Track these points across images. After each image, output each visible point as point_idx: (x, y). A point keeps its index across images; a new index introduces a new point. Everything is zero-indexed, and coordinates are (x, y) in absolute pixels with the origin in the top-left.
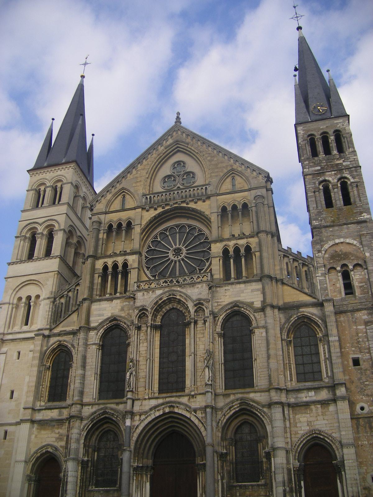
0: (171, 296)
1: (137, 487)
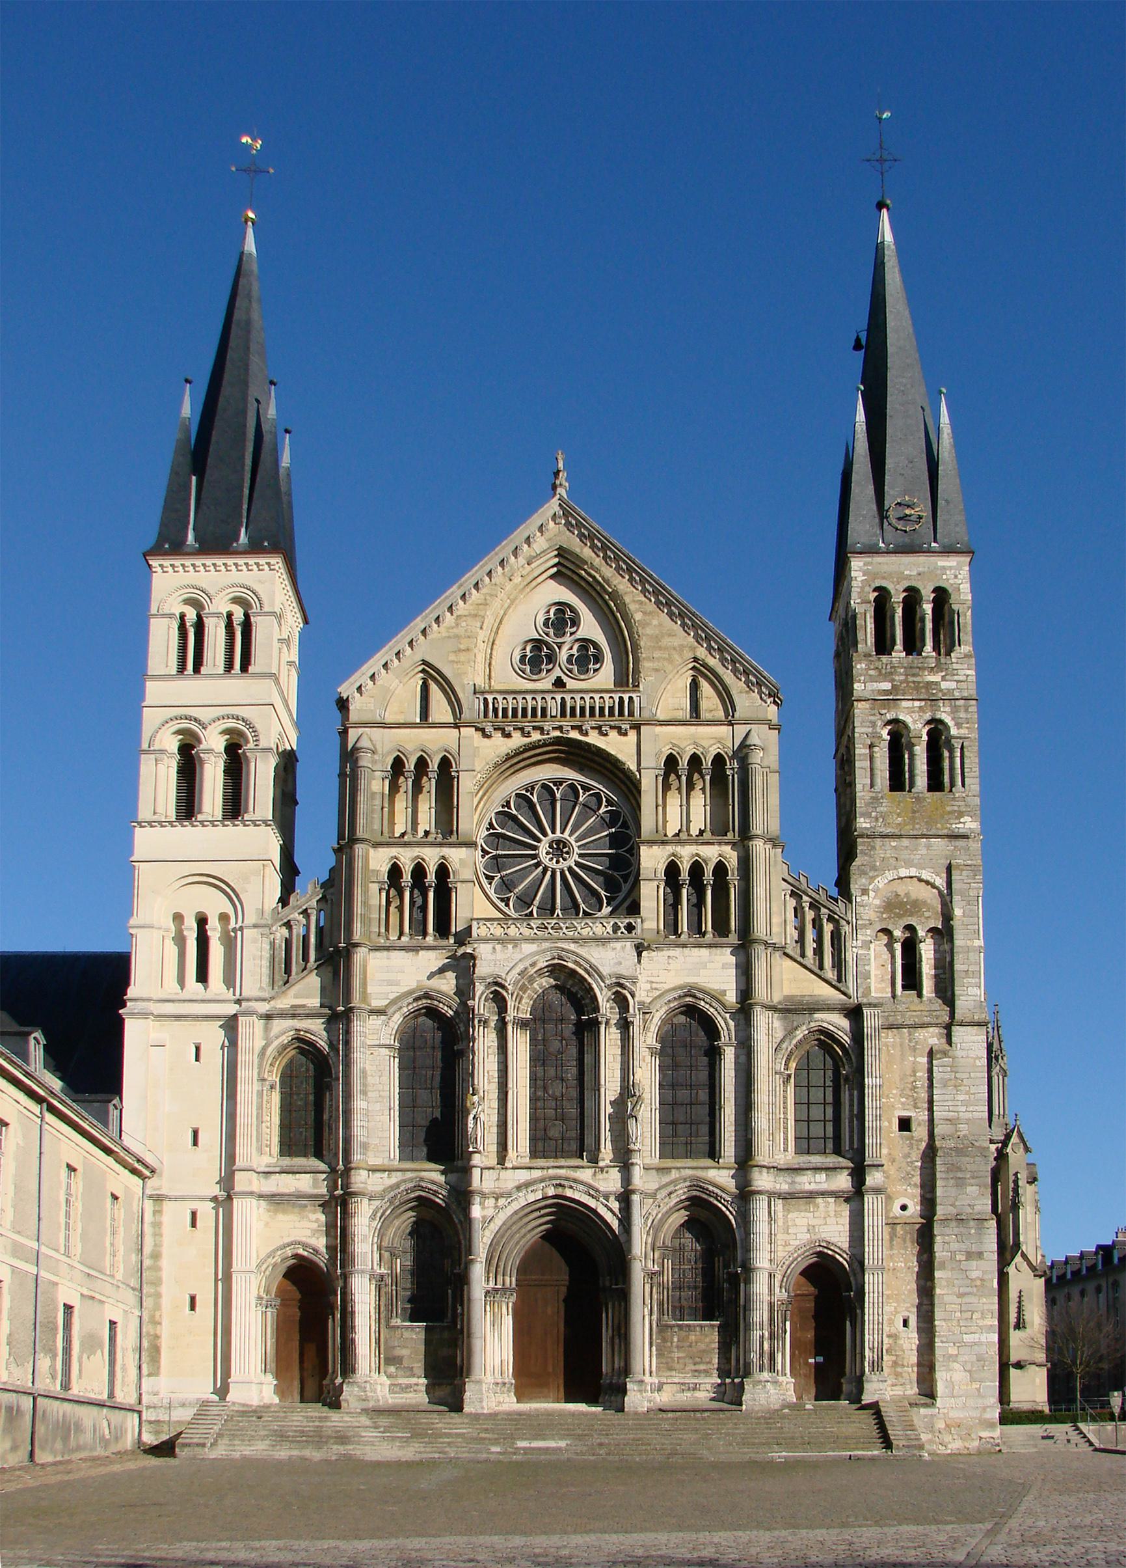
0: (556, 961)
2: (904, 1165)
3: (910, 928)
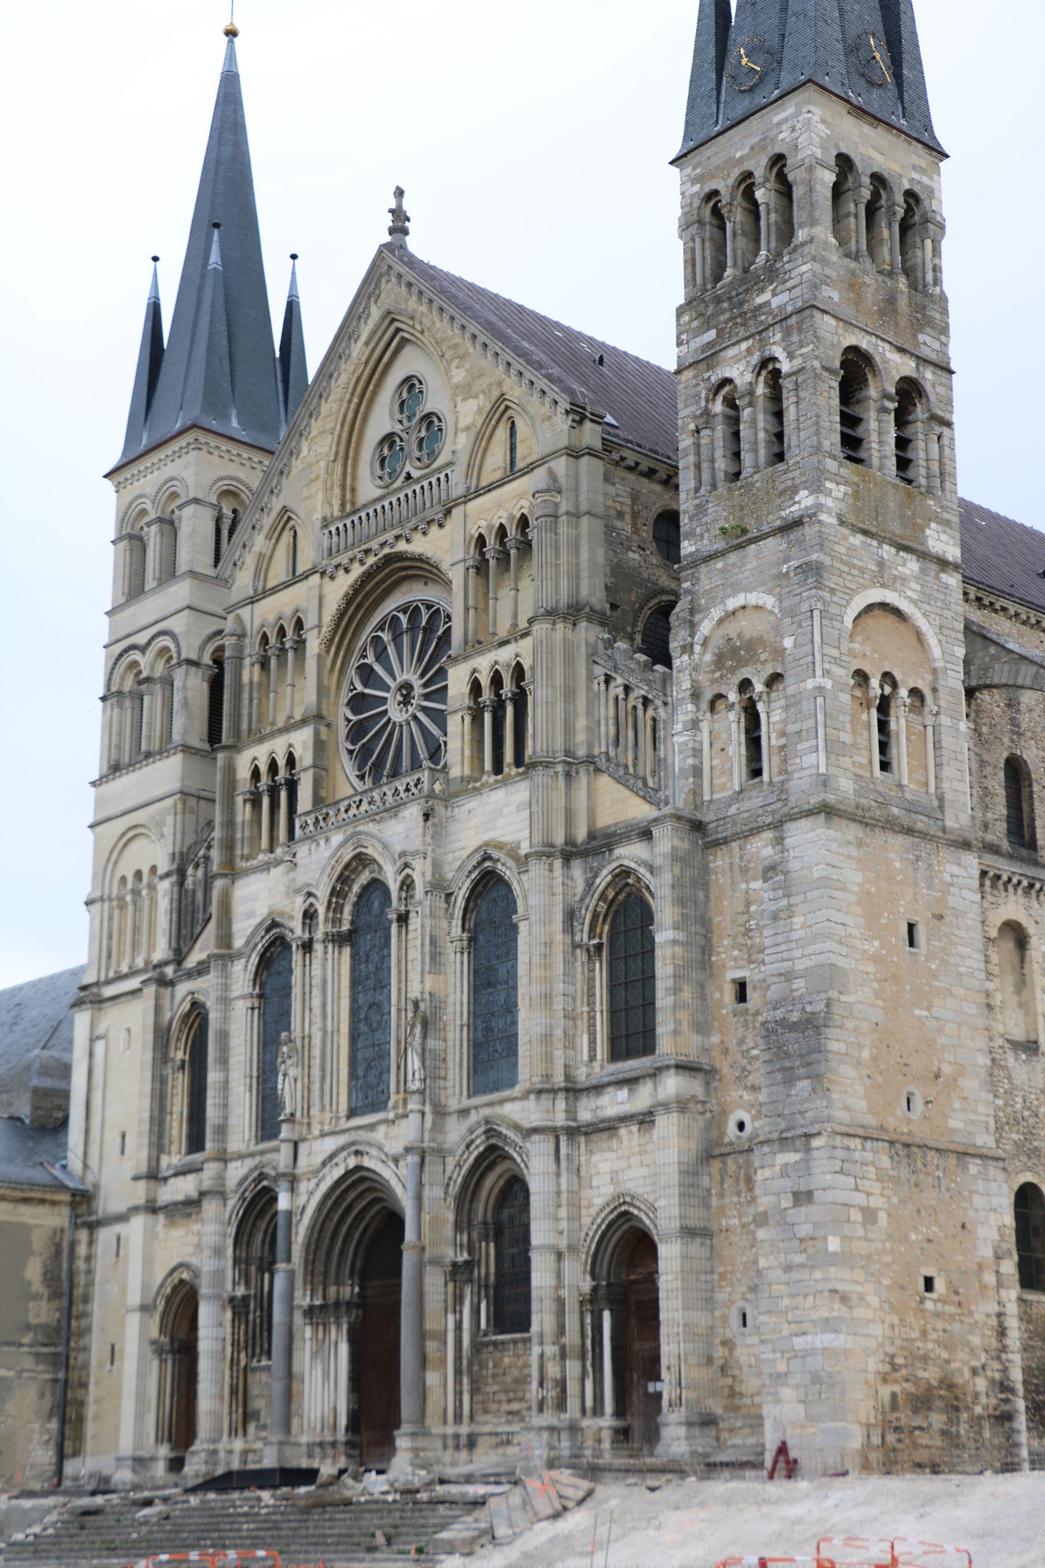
1: (314, 1355)
2: (738, 1056)
3: (745, 685)
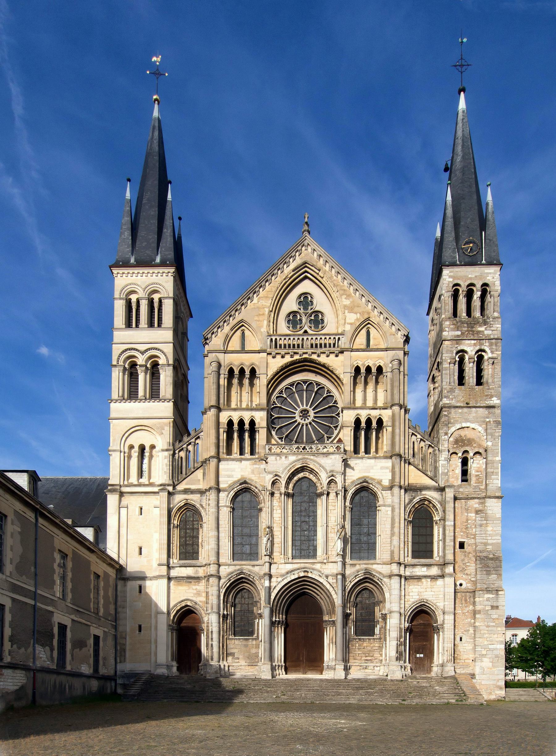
2: (462, 564)
3: (466, 452)
